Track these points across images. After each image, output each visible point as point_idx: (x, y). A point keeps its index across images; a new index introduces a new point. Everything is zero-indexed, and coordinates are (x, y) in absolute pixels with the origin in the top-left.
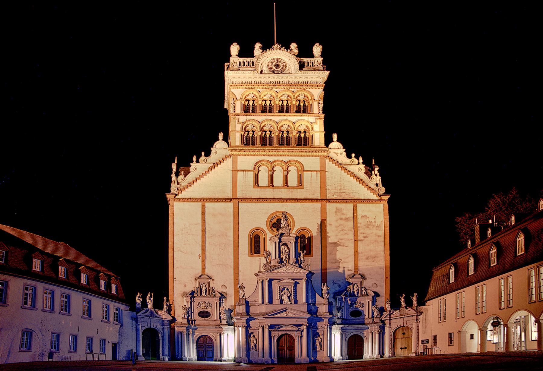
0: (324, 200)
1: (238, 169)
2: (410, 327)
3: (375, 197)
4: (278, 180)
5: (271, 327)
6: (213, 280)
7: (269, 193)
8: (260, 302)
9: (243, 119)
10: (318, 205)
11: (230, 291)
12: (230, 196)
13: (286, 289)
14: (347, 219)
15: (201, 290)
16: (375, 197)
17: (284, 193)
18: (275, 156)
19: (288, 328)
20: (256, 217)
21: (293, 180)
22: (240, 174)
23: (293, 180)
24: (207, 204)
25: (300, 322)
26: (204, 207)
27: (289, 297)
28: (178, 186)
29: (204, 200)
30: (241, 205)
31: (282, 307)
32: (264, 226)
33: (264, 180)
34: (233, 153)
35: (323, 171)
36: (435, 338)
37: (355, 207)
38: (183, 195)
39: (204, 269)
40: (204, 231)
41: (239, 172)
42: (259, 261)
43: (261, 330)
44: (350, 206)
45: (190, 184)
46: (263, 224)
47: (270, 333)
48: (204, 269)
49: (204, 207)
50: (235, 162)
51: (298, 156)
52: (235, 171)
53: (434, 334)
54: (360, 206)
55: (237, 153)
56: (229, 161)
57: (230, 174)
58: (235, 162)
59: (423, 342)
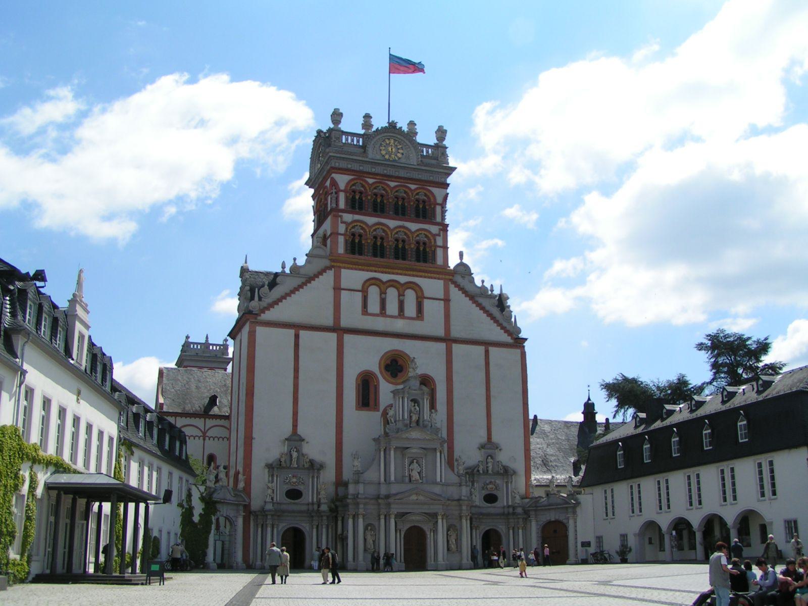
1: (342, 287)
2: (565, 521)
3: (509, 340)
4: (392, 307)
6: (307, 443)
7: (380, 324)
8: (382, 479)
9: (348, 217)
10: (442, 346)
11: (329, 459)
13: (415, 461)
15: (291, 456)
16: (509, 340)
17: (400, 325)
18: (389, 273)
19: (418, 518)
20: (365, 355)
21: (410, 309)
22: (344, 294)
24: (302, 333)
26: (297, 337)
27: (419, 473)
28: (260, 302)
29: (297, 327)
30: (347, 338)
31: (410, 486)
32: (375, 368)
33: (374, 306)
34: (335, 264)
35: (447, 300)
36: (599, 539)
37: (487, 352)
38: (268, 316)
39: (295, 425)
41: (343, 292)
42: (371, 421)
43: (382, 521)
44: (481, 349)
46: (372, 364)
47: (396, 523)
48: (295, 425)
49: (297, 337)
50: (337, 278)
51: (417, 276)
52: (337, 289)
53: (598, 534)
55: (341, 265)
56: (329, 276)
57: (331, 294)
58: (337, 278)
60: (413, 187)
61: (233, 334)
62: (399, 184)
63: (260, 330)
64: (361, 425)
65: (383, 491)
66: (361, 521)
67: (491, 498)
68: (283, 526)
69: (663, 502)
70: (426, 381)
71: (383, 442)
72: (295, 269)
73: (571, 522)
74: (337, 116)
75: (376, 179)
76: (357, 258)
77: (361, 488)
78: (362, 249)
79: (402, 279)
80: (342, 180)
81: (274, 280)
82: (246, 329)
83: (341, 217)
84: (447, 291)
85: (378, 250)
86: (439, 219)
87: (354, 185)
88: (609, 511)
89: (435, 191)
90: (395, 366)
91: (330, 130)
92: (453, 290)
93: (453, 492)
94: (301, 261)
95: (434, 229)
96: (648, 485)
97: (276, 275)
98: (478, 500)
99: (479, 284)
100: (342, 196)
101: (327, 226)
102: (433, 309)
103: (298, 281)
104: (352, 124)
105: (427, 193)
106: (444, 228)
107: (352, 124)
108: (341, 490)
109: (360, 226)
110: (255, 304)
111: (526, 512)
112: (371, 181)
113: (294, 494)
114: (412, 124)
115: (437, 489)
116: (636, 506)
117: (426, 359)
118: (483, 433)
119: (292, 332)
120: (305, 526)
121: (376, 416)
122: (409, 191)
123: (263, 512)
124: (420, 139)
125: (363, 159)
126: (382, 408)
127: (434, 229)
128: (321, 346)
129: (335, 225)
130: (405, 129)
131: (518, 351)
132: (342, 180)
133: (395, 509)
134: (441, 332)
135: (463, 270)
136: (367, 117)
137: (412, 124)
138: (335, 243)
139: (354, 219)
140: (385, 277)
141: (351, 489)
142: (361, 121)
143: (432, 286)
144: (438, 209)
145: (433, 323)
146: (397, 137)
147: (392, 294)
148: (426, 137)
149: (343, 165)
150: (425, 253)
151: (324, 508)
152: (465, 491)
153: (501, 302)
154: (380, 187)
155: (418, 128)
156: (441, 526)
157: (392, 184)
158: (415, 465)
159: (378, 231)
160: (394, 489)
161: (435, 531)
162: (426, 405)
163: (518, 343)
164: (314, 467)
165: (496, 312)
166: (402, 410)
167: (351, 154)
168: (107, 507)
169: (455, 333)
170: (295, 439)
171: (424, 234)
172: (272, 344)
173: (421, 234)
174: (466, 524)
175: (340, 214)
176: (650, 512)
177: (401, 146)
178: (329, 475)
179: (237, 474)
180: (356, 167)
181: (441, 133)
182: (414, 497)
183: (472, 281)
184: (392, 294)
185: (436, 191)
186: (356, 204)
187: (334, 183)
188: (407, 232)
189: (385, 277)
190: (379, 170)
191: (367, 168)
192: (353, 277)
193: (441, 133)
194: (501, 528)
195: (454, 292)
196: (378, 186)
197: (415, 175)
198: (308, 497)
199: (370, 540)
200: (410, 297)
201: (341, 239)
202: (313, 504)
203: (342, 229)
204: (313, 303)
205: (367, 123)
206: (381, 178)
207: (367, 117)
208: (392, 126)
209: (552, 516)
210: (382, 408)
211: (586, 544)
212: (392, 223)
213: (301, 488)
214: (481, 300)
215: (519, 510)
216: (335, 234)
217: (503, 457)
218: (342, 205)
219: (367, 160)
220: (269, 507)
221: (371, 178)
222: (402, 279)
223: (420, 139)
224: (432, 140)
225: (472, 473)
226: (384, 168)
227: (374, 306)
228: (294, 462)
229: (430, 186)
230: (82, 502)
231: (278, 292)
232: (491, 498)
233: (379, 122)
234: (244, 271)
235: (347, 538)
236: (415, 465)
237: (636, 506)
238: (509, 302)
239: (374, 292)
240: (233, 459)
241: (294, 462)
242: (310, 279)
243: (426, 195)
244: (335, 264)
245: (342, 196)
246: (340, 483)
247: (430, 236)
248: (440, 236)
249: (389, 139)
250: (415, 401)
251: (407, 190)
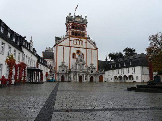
0: (86, 48)
4: (78, 43)
5: (78, 74)
7: (76, 46)
9: (72, 30)
11: (68, 66)
12: (68, 45)
14: (90, 53)
17: (79, 46)
20: (74, 50)
21: (81, 44)
23: (81, 44)
25: (84, 73)
26: (64, 47)
30: (71, 48)
32: (75, 52)
33: (75, 43)
35: (86, 42)
38: (59, 44)
39: (63, 61)
40: (64, 52)
44: (91, 50)
45: (61, 42)
48: (63, 61)
49: (64, 47)
50: (70, 39)
52: (70, 40)
54: (93, 50)
58: (70, 39)
59: (105, 79)
60: (81, 25)
61: (54, 47)
63: (58, 46)
64: (73, 61)
65: (76, 70)
66: (73, 75)
67: (92, 72)
68: (61, 75)
69: (118, 73)
70: (83, 54)
71: (76, 63)
72: (63, 38)
73: (104, 76)
74: (70, 14)
76: (73, 36)
77: (73, 70)
78: (74, 34)
79: (80, 39)
80: (71, 24)
81: (60, 39)
82: (56, 46)
84: (86, 41)
85: (76, 35)
86: (85, 30)
88: (109, 74)
90: (78, 52)
91: (69, 16)
92: (87, 41)
93: (87, 71)
94: (64, 36)
95: (84, 32)
96: (115, 71)
97: (61, 38)
98: (90, 72)
99: (91, 40)
100: (71, 26)
101: (68, 31)
102: (84, 44)
103: (64, 39)
104: (72, 15)
106: (86, 31)
107: (72, 15)
108: (70, 70)
110: (57, 42)
111: (97, 74)
112: (75, 24)
113: (63, 71)
114: (81, 15)
115: (84, 71)
116: (114, 74)
117: (83, 51)
118: (91, 62)
119: (63, 47)
120: (64, 75)
121: (75, 59)
123: (58, 73)
124: (83, 18)
126: (76, 58)
127: (84, 32)
128: (67, 49)
129: (69, 31)
130: (80, 16)
131: (97, 50)
132: (71, 24)
133: (78, 73)
134: (85, 47)
135: (89, 38)
136: (75, 14)
137: (81, 15)
138: (70, 33)
140: (77, 39)
141: (71, 70)
143: (84, 40)
144: (85, 29)
145: (84, 46)
147: (78, 41)
148: (83, 17)
149: (71, 22)
150: (82, 35)
151: (67, 73)
152: (88, 71)
153: (94, 43)
155: (82, 16)
156: (85, 76)
157: (78, 25)
158: (81, 67)
160: (78, 70)
161: (84, 76)
162: (83, 58)
163: (97, 49)
164: (66, 67)
165: (93, 44)
166: (79, 58)
168: (36, 72)
169: (87, 47)
170: (63, 62)
172: (60, 48)
174: (88, 75)
176: (116, 75)
178: (68, 68)
179: (54, 68)
180: (73, 22)
181: (86, 17)
182: (80, 72)
183: (90, 40)
184: (78, 41)
185: (85, 26)
186: (73, 28)
187: (69, 24)
189: (77, 39)
190: (76, 22)
191: (75, 22)
192: (72, 39)
193: (86, 17)
194: (93, 76)
195: (87, 41)
197: (82, 23)
198: (65, 71)
199: (74, 78)
200: (81, 42)
201: (70, 33)
202: (66, 72)
203: (71, 31)
204: (66, 42)
205: (75, 15)
207: (75, 14)
208: (78, 15)
209: (101, 75)
210: (76, 58)
211: (106, 79)
212: (78, 31)
213: (64, 70)
214: (91, 43)
215: (96, 74)
216: (69, 32)
217: (94, 66)
218: (71, 28)
220: (59, 72)
222: (80, 39)
223: (83, 18)
224: (84, 18)
225: (89, 68)
227: (75, 43)
228: (63, 66)
230: (32, 72)
231: (61, 41)
232: (92, 72)
233: (76, 15)
234: (56, 37)
235: (71, 77)
236: (81, 67)
237: (114, 74)
238: (95, 43)
239: (75, 41)
240: (54, 65)
241: (63, 66)
242: (66, 39)
244: (70, 36)
245: (71, 26)
246: (70, 69)
250: (81, 57)
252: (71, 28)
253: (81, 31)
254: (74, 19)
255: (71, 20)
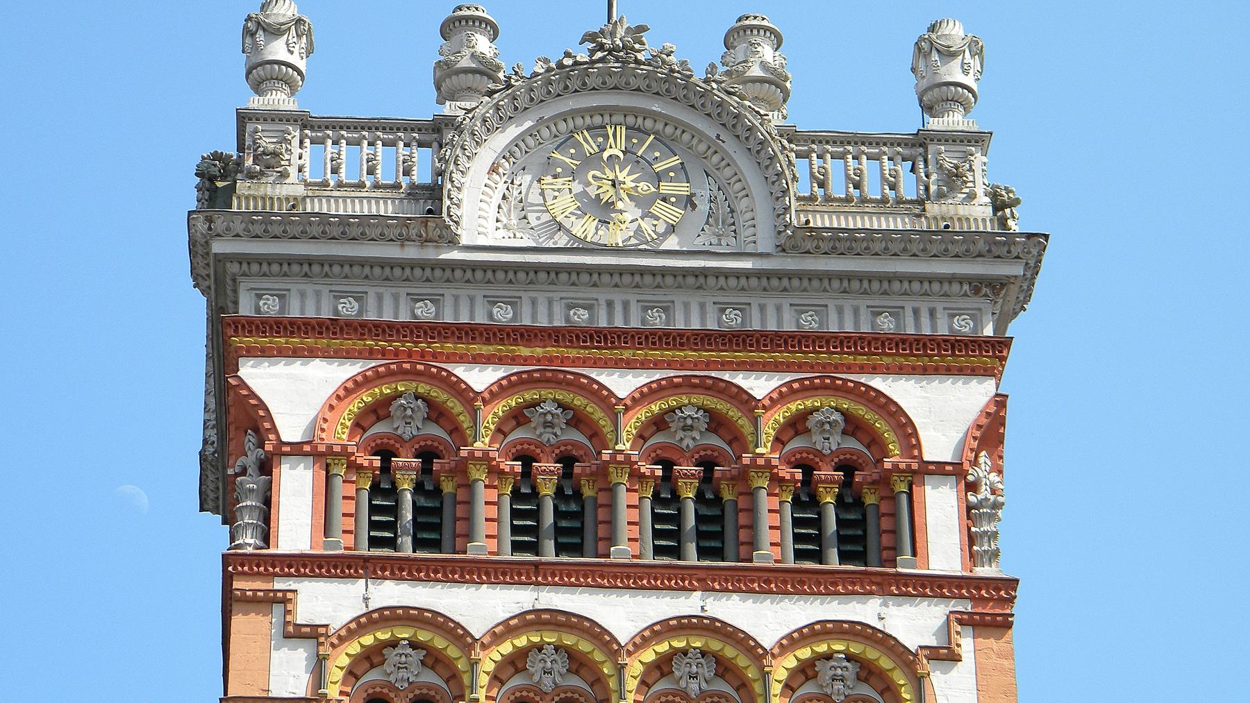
9: (328, 602)
62: (658, 375)
75: (514, 360)
83: (284, 600)
86: (943, 553)
87: (378, 410)
89: (903, 391)
95: (913, 623)
100: (296, 486)
105: (861, 411)
109: (414, 645)
112: (480, 378)
122: (733, 413)
125: (430, 254)
127: (913, 623)
139: (373, 605)
142: (430, 48)
146: (647, 114)
149: (307, 303)
154: (548, 407)
159: (535, 665)
167: (346, 228)
171: (850, 657)
173: (828, 657)
175: (279, 584)
177: (674, 161)
180: (389, 307)
188: (730, 652)
190: (543, 311)
196: (534, 404)
206: (552, 350)
219: (456, 255)
221: (477, 360)
226: (571, 293)
229: (875, 370)
243: (853, 426)
247: (885, 663)
248: (954, 658)
249: (597, 130)
251: (721, 405)
252: (295, 531)
253: (734, 610)
254: (432, 195)
255: (321, 247)
